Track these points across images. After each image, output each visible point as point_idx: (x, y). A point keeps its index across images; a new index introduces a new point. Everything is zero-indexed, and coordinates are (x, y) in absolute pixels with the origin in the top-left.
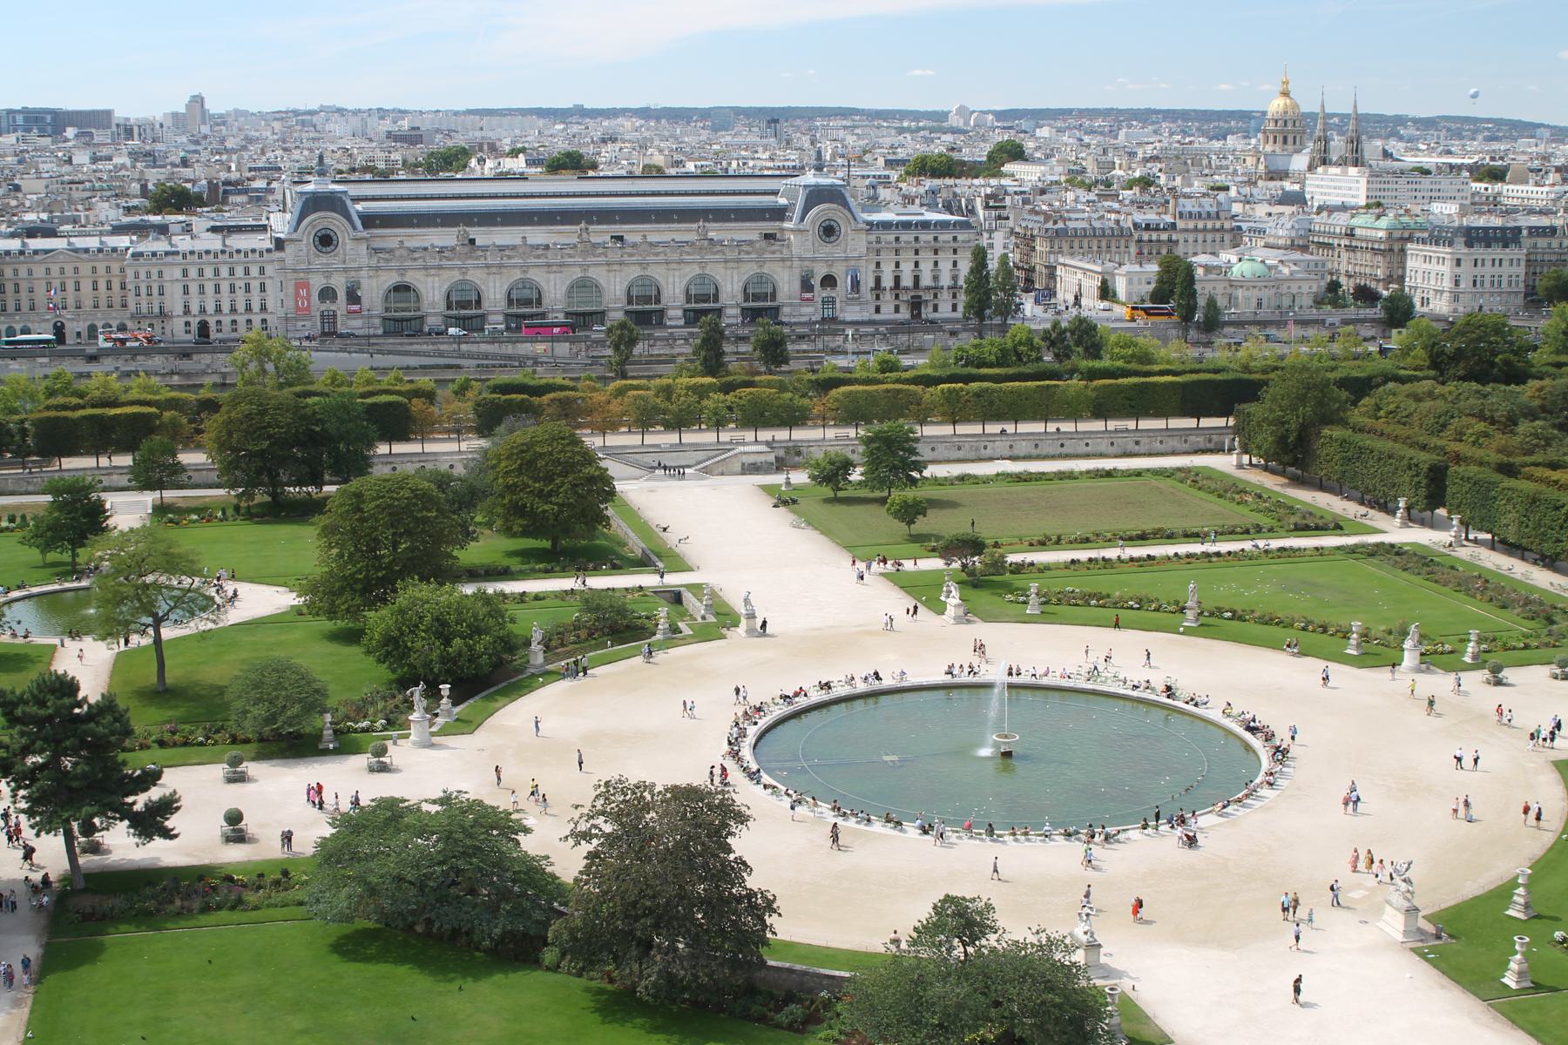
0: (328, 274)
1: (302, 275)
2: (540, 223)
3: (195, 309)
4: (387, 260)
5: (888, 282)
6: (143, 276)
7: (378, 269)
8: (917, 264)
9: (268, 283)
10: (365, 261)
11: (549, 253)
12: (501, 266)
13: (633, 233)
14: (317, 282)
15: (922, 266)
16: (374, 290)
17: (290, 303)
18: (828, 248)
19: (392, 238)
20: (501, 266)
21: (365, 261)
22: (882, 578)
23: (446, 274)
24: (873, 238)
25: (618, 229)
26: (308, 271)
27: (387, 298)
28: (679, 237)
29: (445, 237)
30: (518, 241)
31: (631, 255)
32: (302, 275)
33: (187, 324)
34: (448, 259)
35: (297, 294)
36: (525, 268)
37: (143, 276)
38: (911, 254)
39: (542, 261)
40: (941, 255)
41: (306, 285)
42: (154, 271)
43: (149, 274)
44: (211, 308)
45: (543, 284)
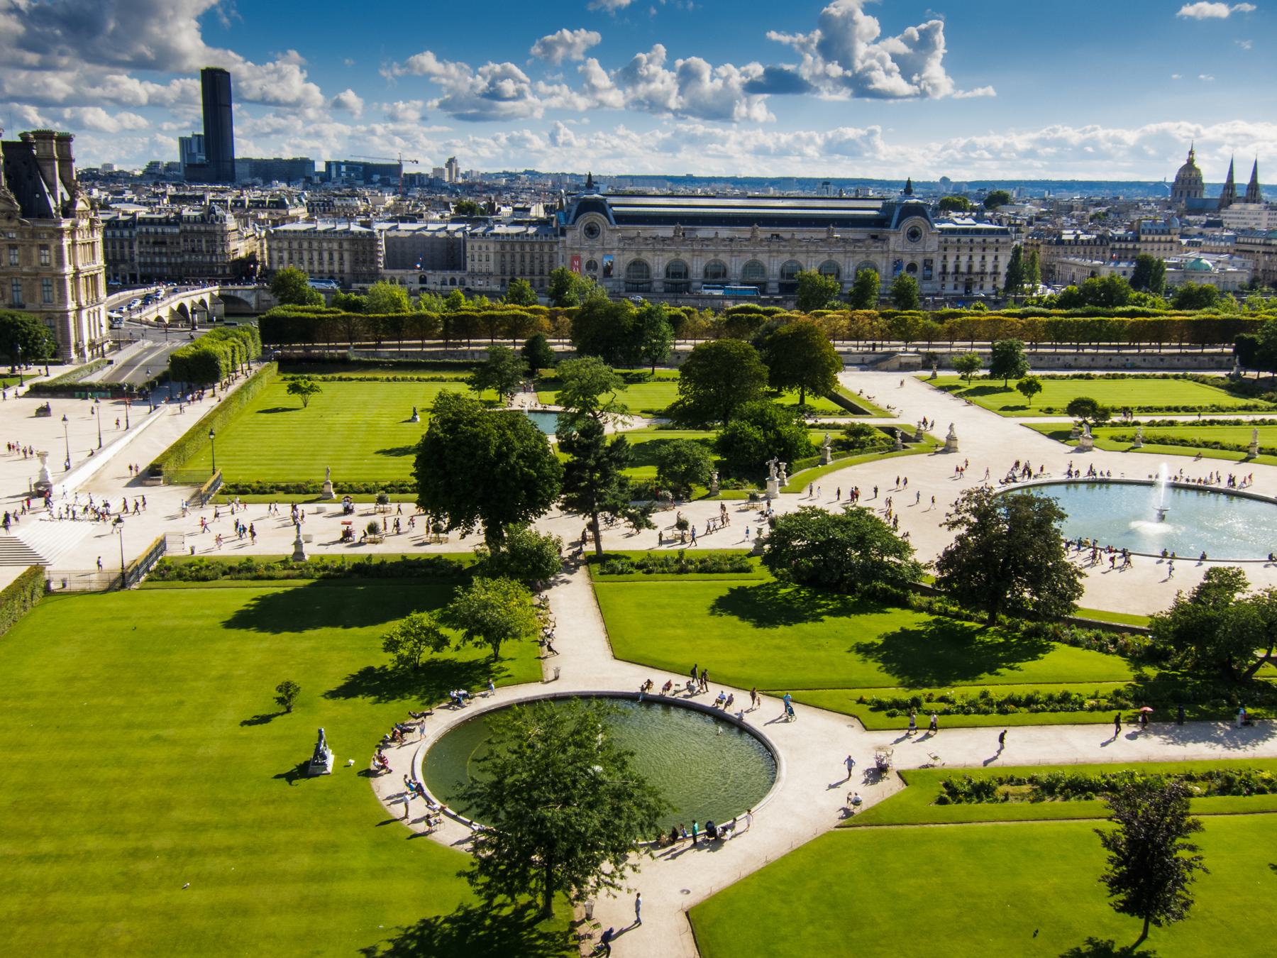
0: (592, 252)
1: (576, 252)
2: (726, 224)
4: (629, 244)
5: (951, 268)
6: (476, 248)
7: (624, 250)
8: (971, 257)
10: (616, 244)
11: (733, 244)
12: (701, 251)
13: (785, 232)
14: (585, 257)
15: (975, 259)
18: (913, 245)
19: (633, 230)
20: (701, 251)
21: (616, 244)
23: (667, 255)
24: (942, 239)
25: (775, 230)
26: (580, 249)
27: (628, 269)
28: (815, 235)
30: (712, 235)
31: (785, 246)
32: (576, 252)
34: (669, 245)
36: (716, 253)
37: (476, 248)
38: (967, 251)
39: (728, 248)
40: (988, 251)
41: (578, 258)
42: (484, 245)
43: (480, 248)
45: (728, 263)
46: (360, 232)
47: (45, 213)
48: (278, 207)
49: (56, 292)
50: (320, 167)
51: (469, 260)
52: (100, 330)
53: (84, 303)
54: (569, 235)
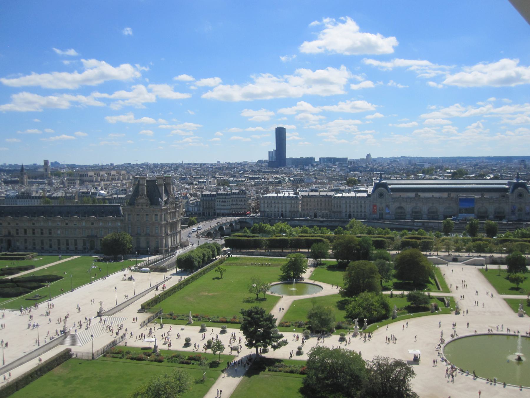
22: (505, 302)
29: (412, 195)
33: (346, 214)
35: (373, 209)
46: (293, 197)
47: (158, 204)
48: (278, 183)
49: (159, 230)
50: (317, 160)
52: (174, 243)
53: (169, 233)
54: (372, 197)
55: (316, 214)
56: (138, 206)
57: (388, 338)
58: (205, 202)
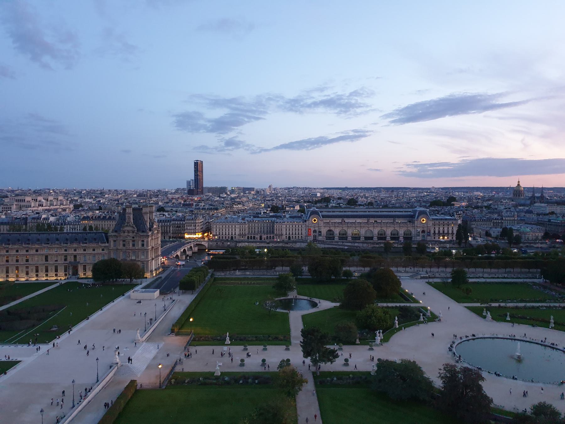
1: (309, 227)
3: (288, 233)
5: (437, 232)
8: (444, 228)
9: (303, 229)
13: (379, 220)
15: (445, 228)
16: (324, 231)
17: (307, 234)
20: (351, 227)
24: (433, 222)
25: (376, 219)
28: (389, 221)
33: (286, 237)
41: (310, 229)
43: (279, 226)
44: (291, 234)
51: (275, 230)
55: (261, 236)
56: (124, 232)
57: (455, 335)
58: (166, 228)
